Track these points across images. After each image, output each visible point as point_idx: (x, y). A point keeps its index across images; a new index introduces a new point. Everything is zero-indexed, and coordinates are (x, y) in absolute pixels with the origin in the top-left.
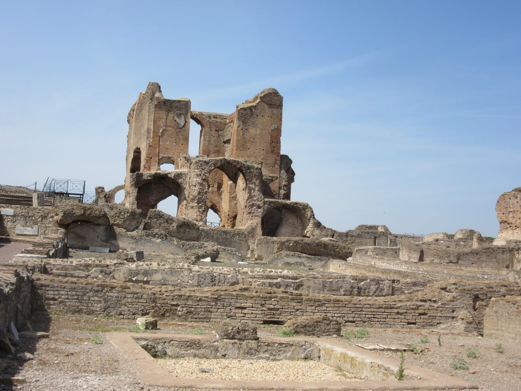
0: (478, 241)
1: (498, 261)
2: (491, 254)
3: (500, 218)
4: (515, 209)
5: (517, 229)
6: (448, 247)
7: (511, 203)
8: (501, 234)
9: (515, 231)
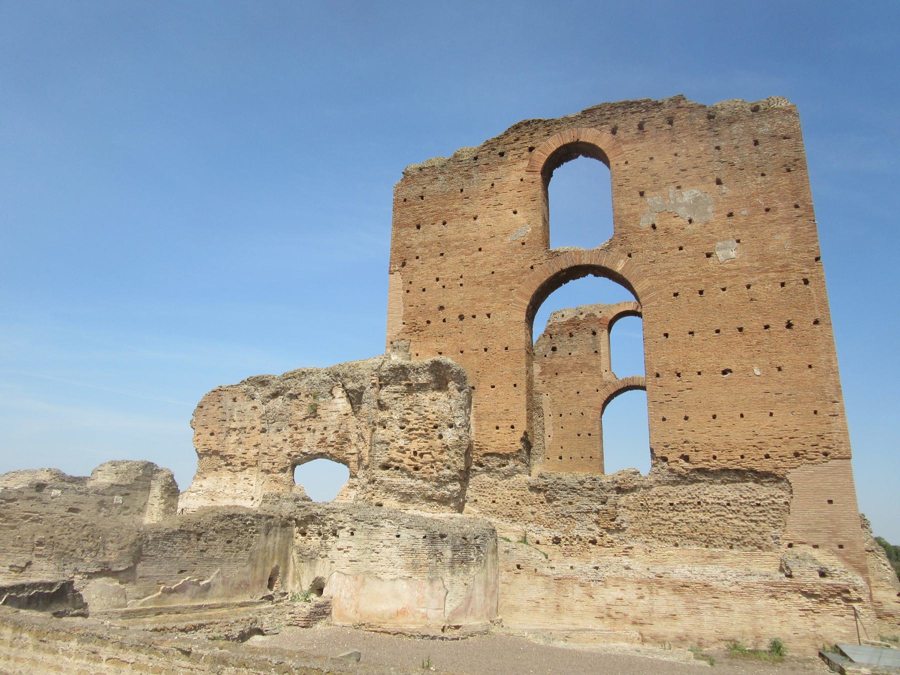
0: (166, 496)
1: (254, 557)
2: (239, 534)
3: (201, 443)
4: (246, 423)
5: (247, 471)
6: (72, 510)
7: (236, 409)
8: (199, 483)
9: (239, 475)
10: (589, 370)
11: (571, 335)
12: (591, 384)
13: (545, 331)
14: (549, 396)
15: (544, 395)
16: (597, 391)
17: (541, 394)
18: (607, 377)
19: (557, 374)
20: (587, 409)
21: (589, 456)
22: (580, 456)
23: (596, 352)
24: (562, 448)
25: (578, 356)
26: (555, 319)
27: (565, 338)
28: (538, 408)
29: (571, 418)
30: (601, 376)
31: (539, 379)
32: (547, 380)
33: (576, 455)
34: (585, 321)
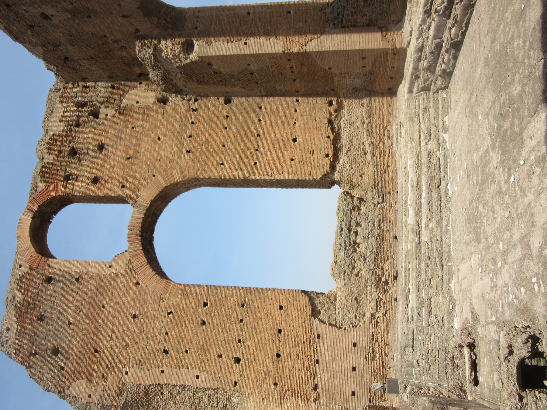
10: (102, 294)
11: (41, 319)
12: (127, 293)
13: (22, 363)
14: (130, 371)
15: (127, 379)
16: (138, 284)
17: (123, 384)
18: (120, 267)
19: (96, 351)
20: (163, 305)
21: (240, 309)
22: (238, 325)
23: (77, 280)
24: (220, 356)
25: (78, 311)
26: (9, 343)
27: (42, 328)
28: (147, 393)
29: (173, 333)
30: (117, 275)
31: (97, 385)
32: (103, 370)
33: (235, 331)
34: (26, 291)
